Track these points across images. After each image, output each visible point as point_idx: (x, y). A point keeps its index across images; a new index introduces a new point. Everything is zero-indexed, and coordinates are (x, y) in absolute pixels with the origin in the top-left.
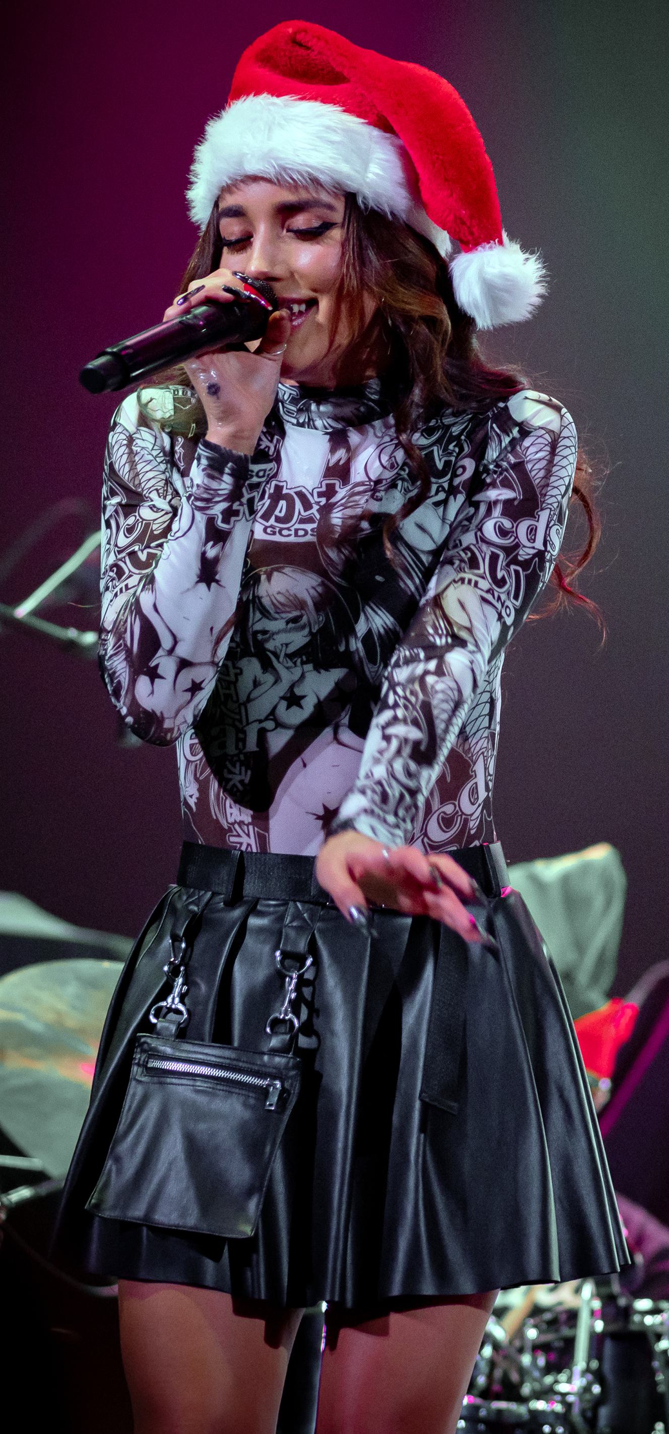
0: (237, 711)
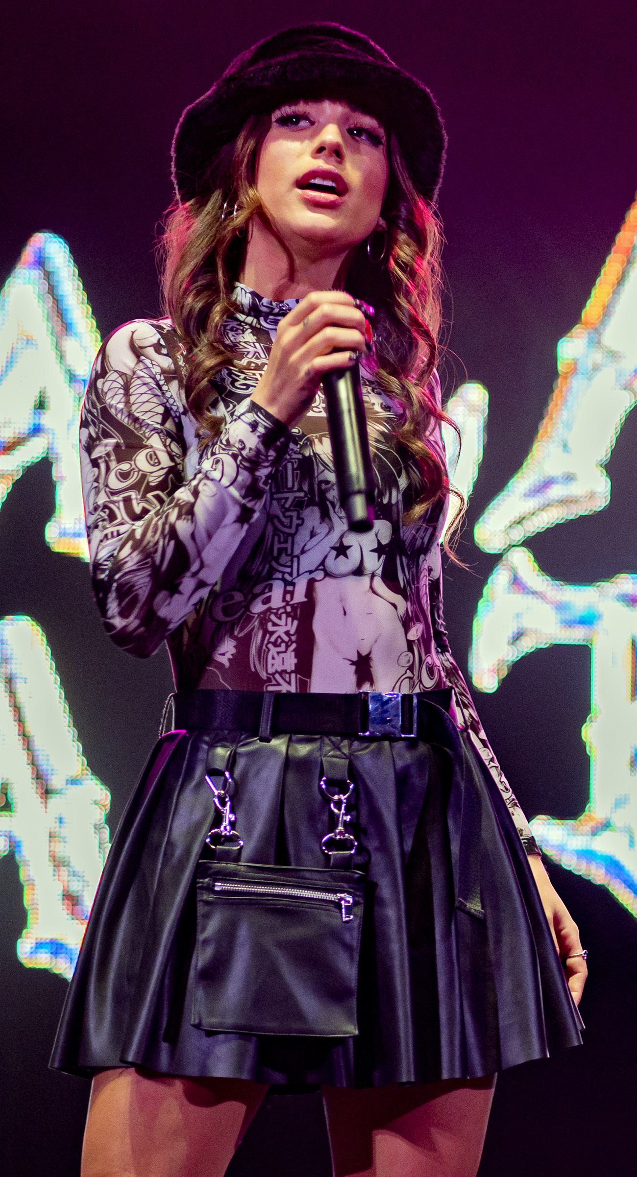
0: (289, 564)
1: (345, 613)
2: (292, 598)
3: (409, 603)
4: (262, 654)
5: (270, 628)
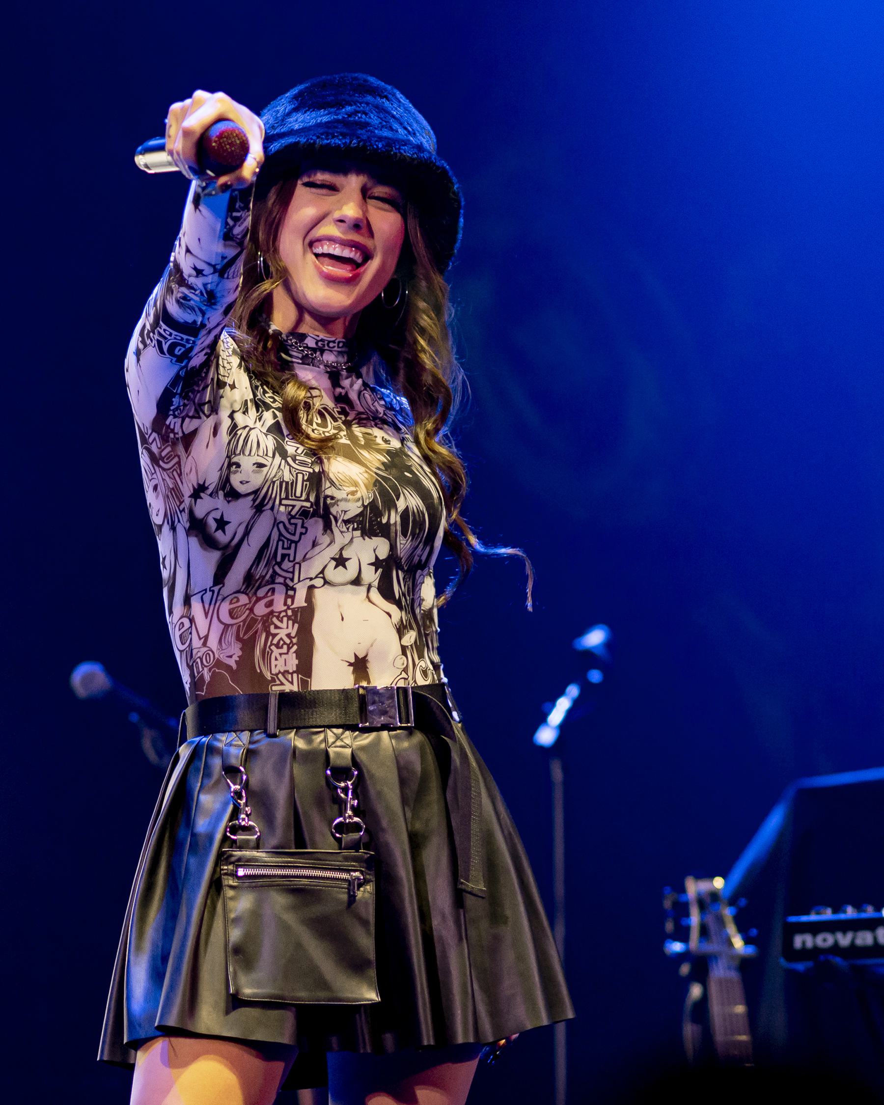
0: (291, 570)
1: (343, 619)
2: (293, 603)
3: (404, 613)
4: (266, 654)
5: (273, 630)
